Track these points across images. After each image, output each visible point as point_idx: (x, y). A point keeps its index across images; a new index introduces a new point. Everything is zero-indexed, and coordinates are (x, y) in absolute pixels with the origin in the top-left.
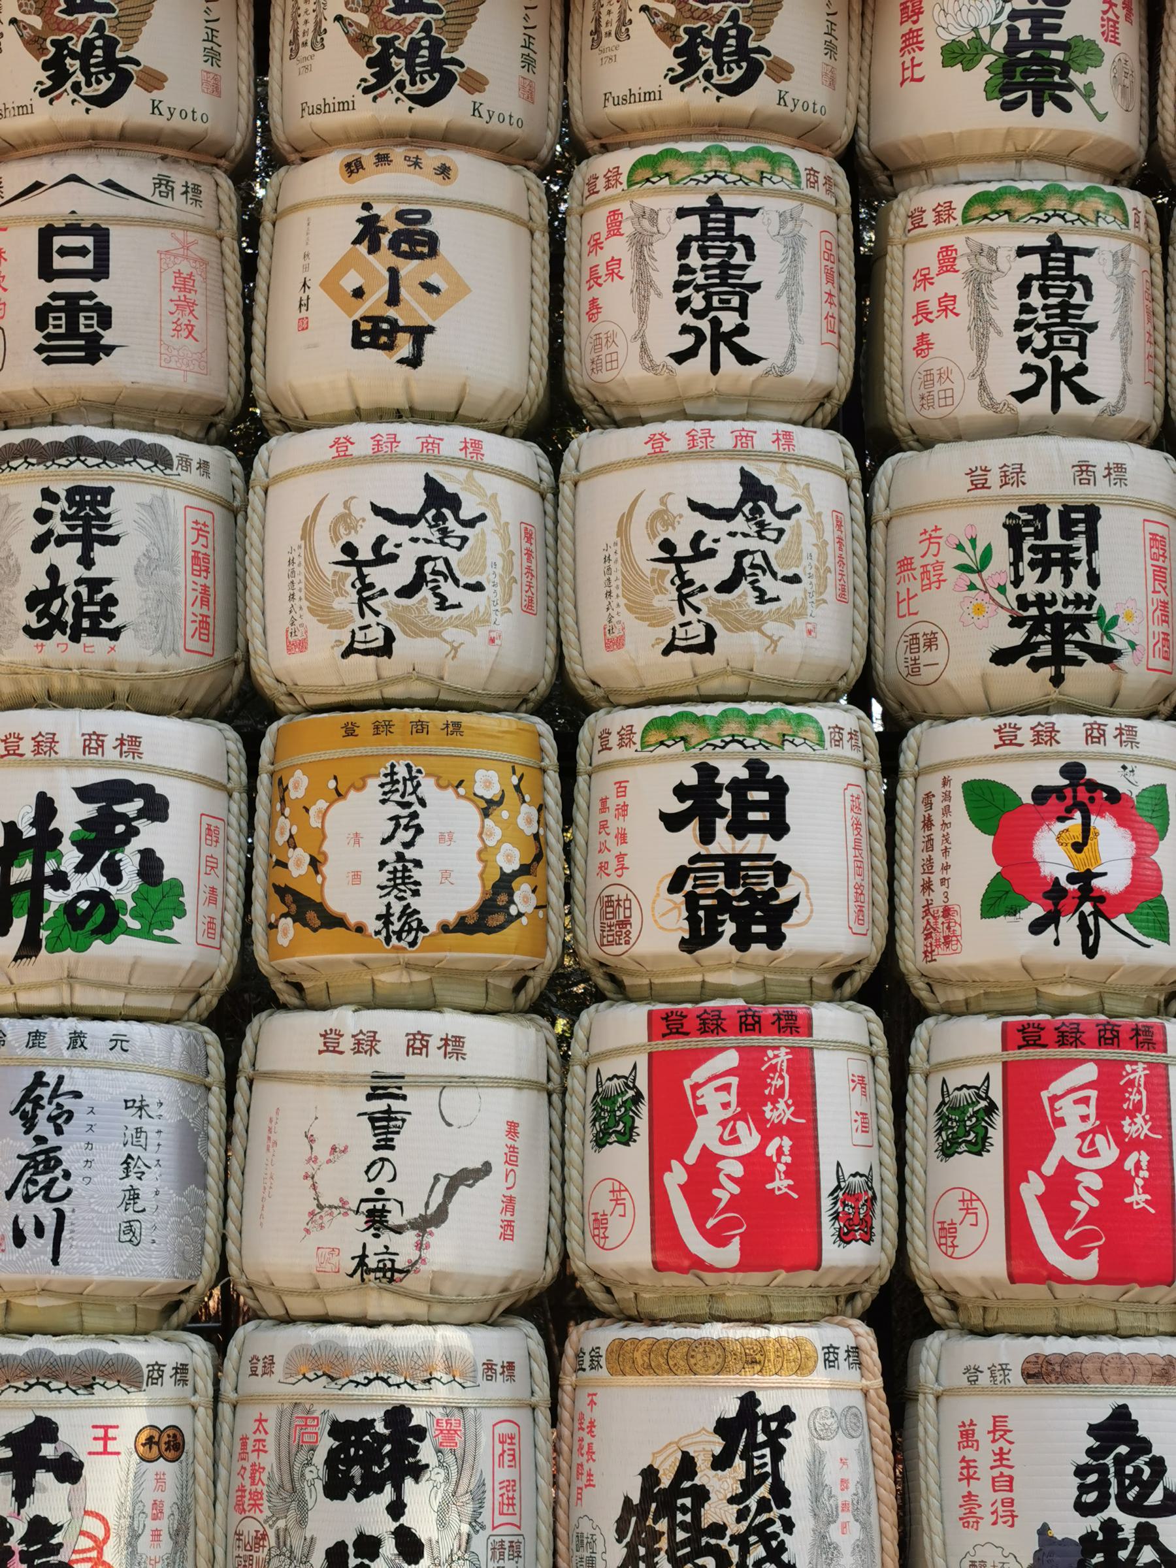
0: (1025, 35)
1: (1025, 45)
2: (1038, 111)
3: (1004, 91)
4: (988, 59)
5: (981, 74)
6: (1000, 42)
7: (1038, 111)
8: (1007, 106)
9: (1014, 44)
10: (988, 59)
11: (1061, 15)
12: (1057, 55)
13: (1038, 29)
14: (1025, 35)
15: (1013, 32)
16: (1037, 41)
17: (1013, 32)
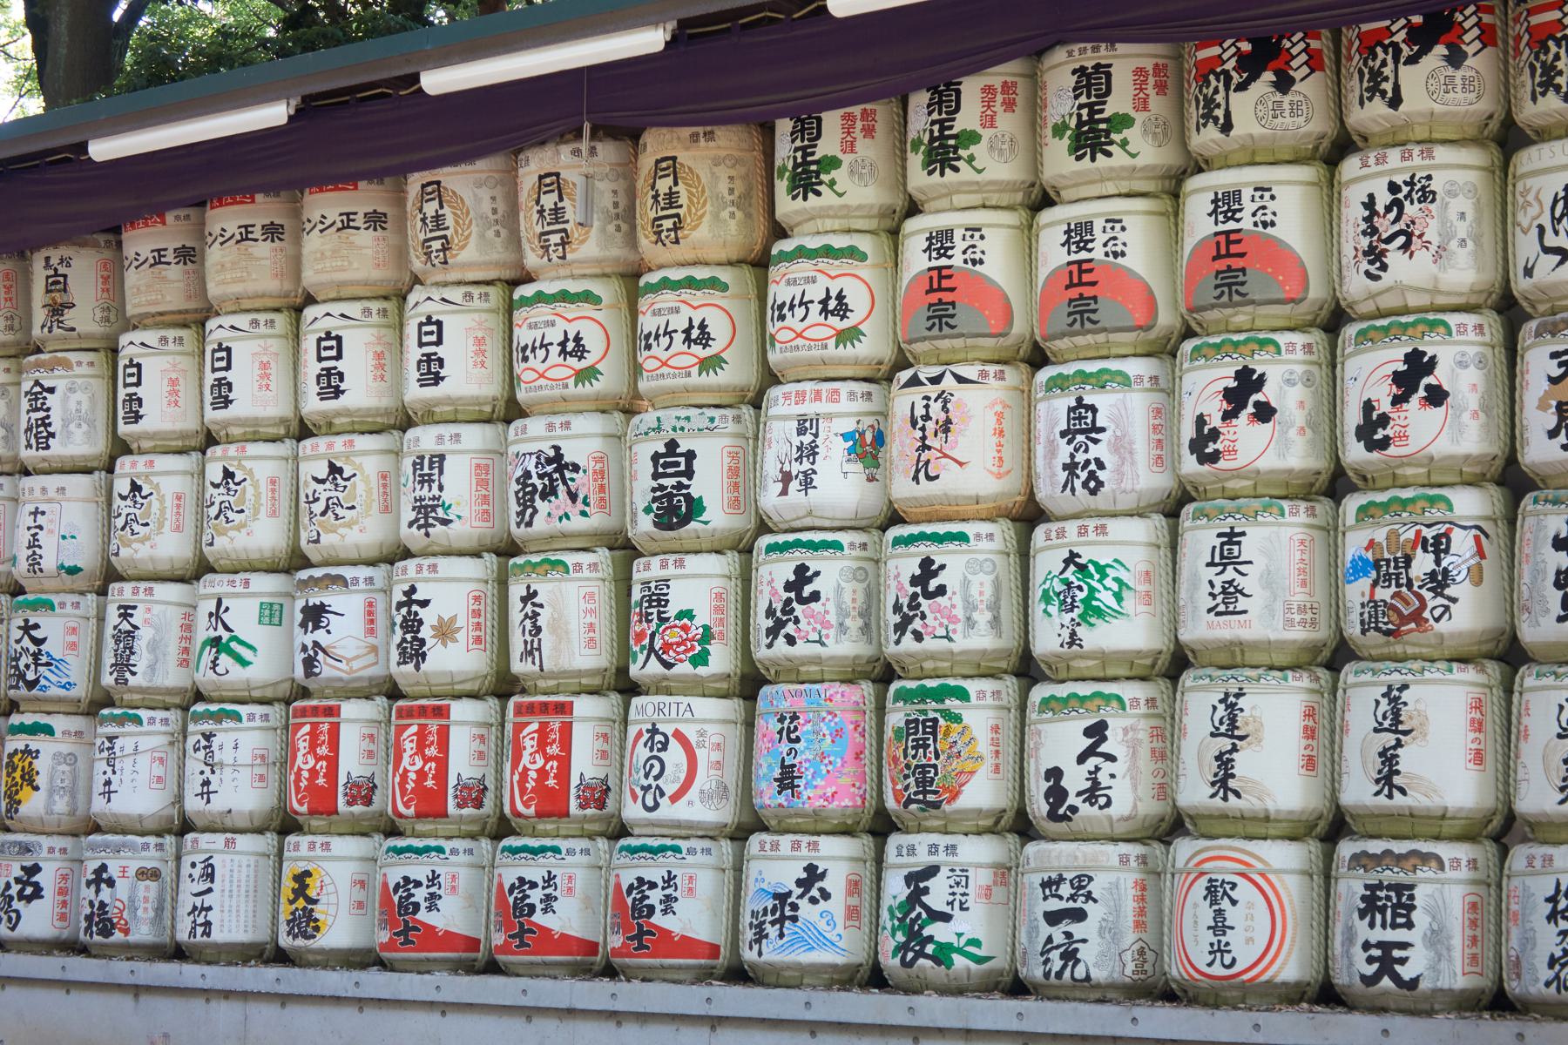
0: (1085, 118)
1: (1085, 123)
2: (1093, 159)
3: (1077, 150)
4: (1069, 133)
5: (1066, 142)
6: (1073, 123)
7: (1093, 159)
8: (1078, 158)
9: (1080, 124)
10: (1069, 133)
11: (1104, 103)
12: (1103, 126)
13: (1092, 113)
14: (1085, 118)
15: (1080, 116)
16: (1092, 120)
17: (1080, 116)
